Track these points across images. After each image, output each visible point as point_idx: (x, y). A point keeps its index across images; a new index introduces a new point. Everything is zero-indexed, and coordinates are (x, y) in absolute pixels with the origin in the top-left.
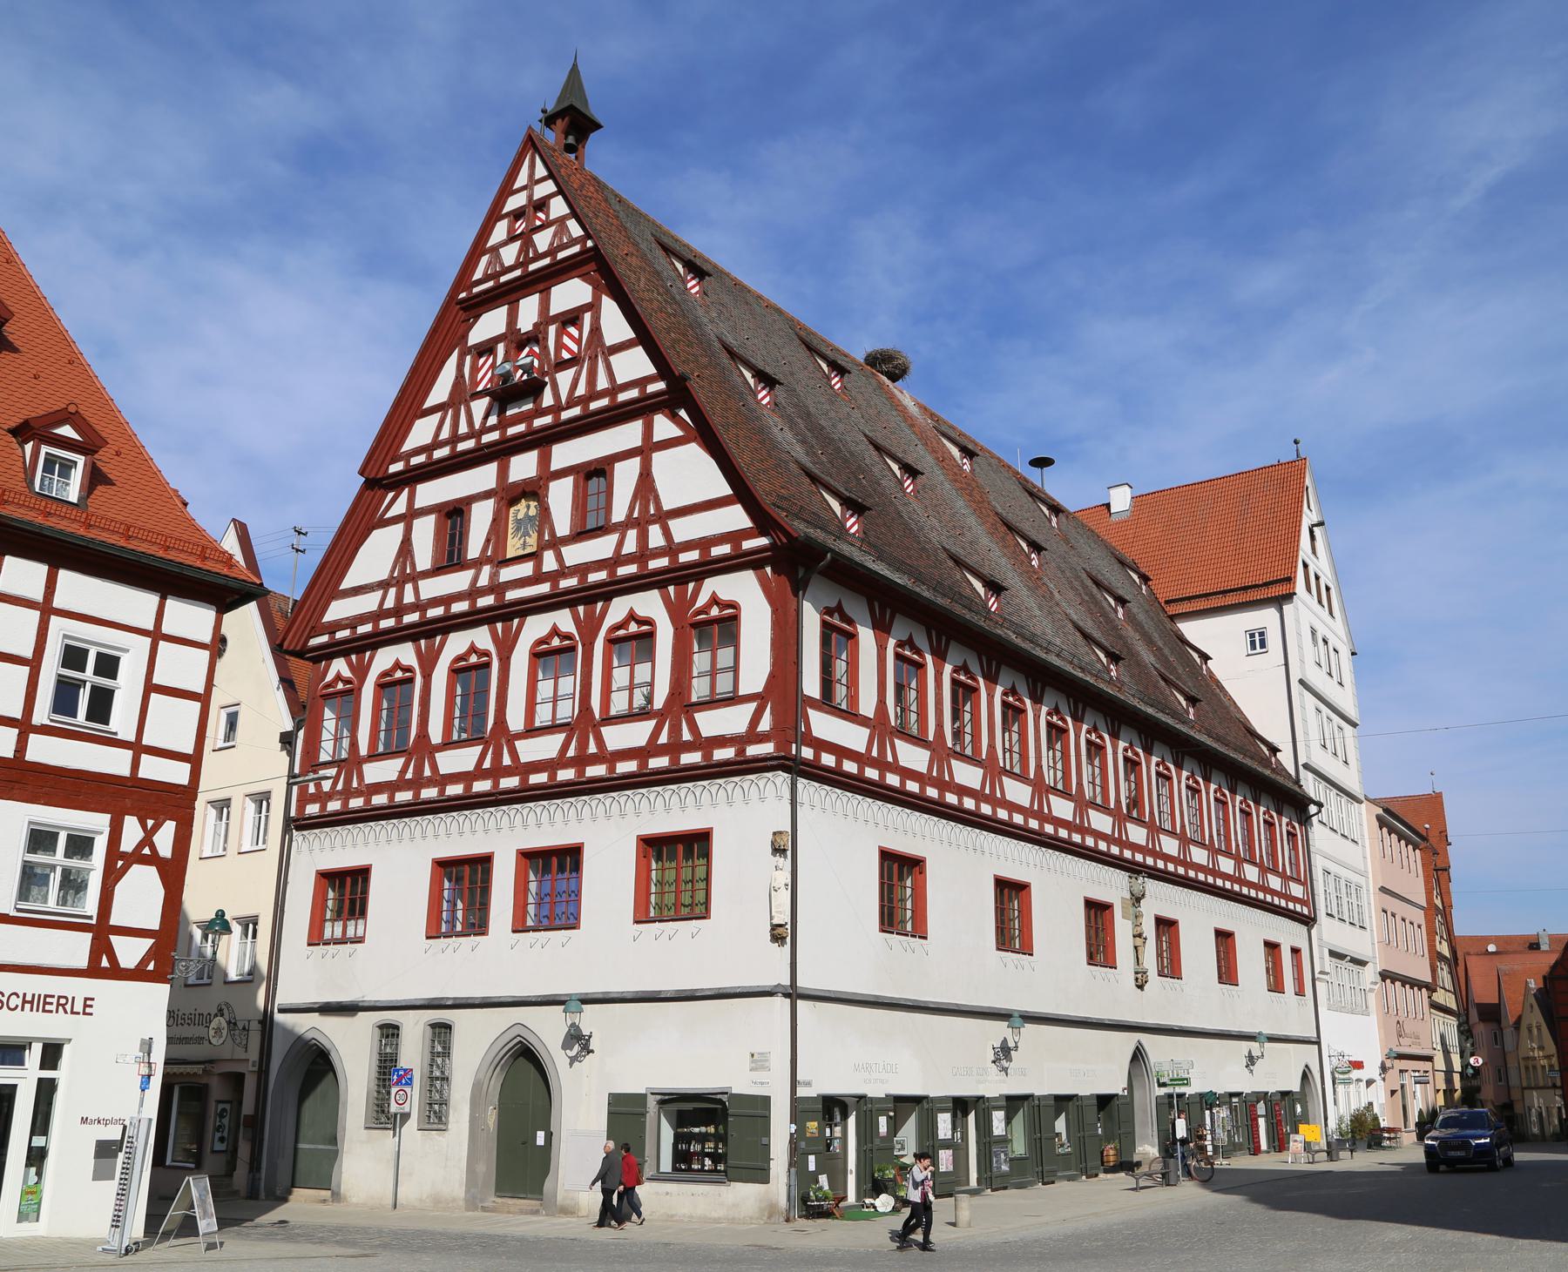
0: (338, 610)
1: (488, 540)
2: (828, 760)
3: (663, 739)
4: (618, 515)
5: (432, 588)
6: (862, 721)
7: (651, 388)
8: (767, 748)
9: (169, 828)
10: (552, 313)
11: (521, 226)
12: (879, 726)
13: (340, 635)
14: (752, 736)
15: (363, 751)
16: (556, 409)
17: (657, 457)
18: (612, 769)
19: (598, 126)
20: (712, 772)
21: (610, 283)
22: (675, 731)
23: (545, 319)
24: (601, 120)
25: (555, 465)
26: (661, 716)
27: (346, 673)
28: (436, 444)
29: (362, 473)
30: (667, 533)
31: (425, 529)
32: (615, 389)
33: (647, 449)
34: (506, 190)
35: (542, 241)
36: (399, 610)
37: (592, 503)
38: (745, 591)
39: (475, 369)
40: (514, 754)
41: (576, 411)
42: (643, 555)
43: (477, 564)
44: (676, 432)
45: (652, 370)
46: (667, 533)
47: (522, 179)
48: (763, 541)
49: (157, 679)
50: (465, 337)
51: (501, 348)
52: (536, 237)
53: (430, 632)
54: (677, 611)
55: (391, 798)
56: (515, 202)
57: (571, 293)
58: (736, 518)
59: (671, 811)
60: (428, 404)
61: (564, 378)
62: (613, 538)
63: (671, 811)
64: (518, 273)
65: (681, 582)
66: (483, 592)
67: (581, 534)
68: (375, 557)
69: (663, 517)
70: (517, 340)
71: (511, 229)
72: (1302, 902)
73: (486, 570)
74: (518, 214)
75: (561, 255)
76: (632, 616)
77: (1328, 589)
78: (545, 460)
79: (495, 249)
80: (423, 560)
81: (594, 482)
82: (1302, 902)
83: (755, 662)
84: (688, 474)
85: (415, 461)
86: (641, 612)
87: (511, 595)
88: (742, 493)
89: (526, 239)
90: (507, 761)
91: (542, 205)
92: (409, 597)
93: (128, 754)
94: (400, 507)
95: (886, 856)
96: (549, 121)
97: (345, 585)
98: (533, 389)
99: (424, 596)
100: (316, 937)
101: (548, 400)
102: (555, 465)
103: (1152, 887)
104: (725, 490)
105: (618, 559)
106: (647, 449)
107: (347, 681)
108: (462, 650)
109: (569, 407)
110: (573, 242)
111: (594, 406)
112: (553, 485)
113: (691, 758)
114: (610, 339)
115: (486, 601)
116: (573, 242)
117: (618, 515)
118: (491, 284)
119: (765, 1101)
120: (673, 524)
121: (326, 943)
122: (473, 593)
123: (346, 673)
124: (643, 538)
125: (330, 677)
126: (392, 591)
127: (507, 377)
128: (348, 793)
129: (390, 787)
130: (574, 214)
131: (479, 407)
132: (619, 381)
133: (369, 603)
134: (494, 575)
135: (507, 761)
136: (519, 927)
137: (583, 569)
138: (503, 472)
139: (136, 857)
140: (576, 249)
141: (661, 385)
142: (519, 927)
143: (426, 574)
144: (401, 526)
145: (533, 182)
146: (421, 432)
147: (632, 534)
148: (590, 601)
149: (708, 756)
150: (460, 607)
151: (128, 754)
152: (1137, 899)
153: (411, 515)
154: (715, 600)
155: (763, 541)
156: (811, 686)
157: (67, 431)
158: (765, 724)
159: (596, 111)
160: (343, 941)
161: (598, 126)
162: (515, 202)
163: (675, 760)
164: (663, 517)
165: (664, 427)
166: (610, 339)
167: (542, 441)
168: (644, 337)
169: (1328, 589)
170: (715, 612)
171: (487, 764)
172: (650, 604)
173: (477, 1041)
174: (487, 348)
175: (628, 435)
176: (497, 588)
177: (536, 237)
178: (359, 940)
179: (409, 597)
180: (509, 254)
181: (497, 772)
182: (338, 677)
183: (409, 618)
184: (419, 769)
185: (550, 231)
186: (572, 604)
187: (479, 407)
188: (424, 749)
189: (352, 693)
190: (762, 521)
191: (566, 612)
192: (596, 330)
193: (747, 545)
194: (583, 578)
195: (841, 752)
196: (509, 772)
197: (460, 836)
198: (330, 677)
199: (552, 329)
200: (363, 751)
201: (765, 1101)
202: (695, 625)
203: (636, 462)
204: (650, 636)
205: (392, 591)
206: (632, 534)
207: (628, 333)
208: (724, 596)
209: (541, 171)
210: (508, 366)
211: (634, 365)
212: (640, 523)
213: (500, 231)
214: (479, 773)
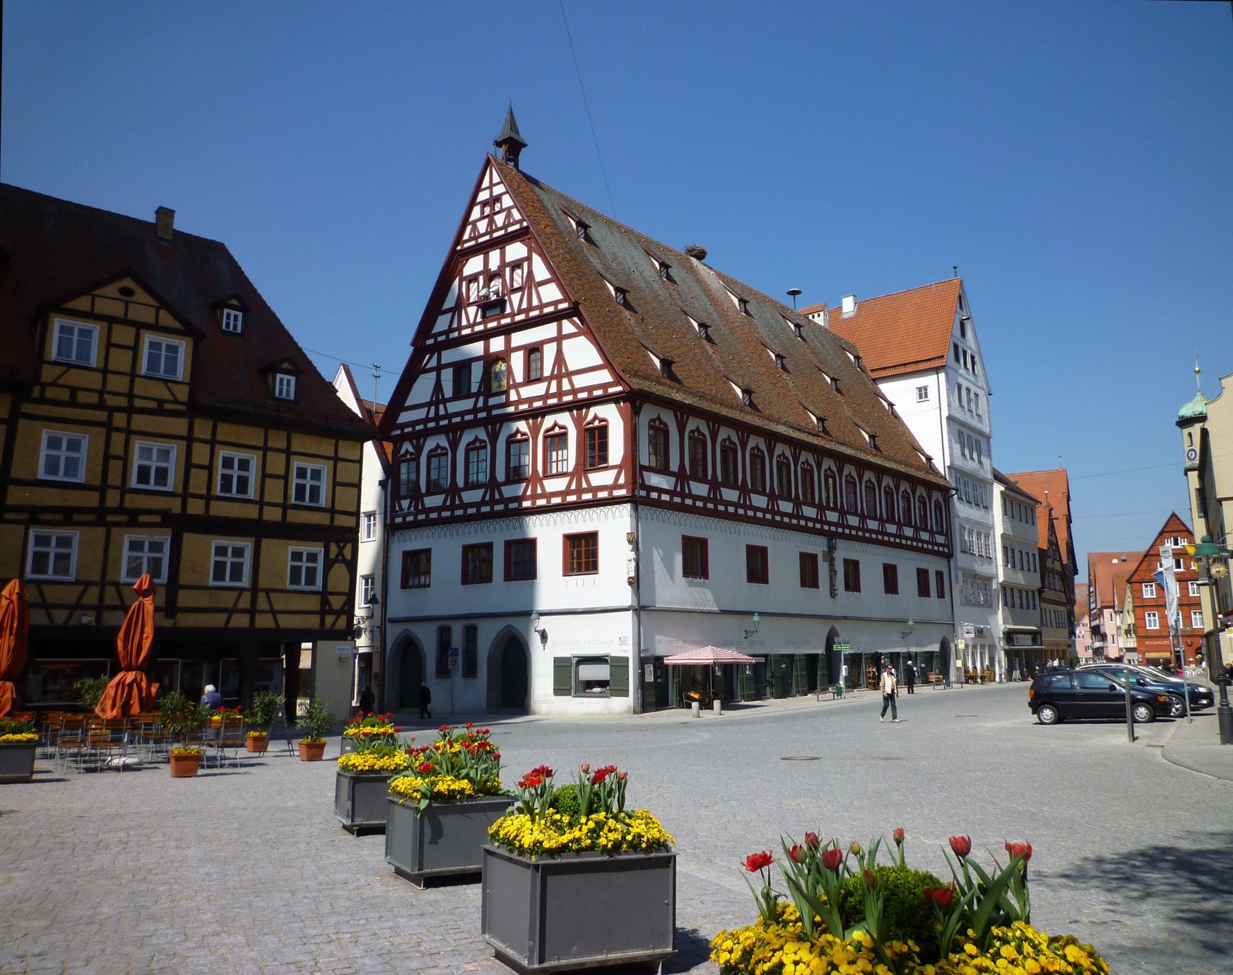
0: (404, 417)
1: (481, 383)
2: (654, 495)
3: (573, 487)
4: (547, 372)
5: (453, 407)
6: (672, 474)
7: (561, 306)
8: (623, 492)
9: (349, 546)
10: (507, 260)
11: (487, 210)
12: (681, 476)
13: (407, 430)
14: (616, 486)
15: (423, 491)
16: (513, 315)
17: (564, 342)
18: (549, 501)
19: (525, 145)
20: (596, 503)
21: (536, 246)
22: (579, 483)
23: (503, 264)
24: (526, 142)
25: (513, 345)
26: (572, 475)
27: (411, 450)
28: (451, 330)
29: (412, 345)
30: (571, 383)
31: (447, 375)
32: (542, 306)
33: (560, 338)
34: (478, 189)
35: (500, 220)
36: (437, 418)
37: (533, 366)
38: (612, 415)
39: (468, 289)
40: (500, 493)
41: (522, 317)
42: (560, 393)
43: (477, 395)
44: (575, 330)
45: (560, 296)
46: (571, 383)
47: (486, 183)
48: (620, 388)
49: (338, 480)
50: (461, 271)
51: (481, 278)
52: (496, 217)
53: (454, 431)
54: (578, 422)
55: (439, 515)
56: (484, 195)
57: (516, 251)
58: (605, 376)
59: (579, 522)
60: (444, 308)
61: (516, 298)
62: (545, 384)
63: (579, 522)
64: (487, 238)
65: (579, 408)
66: (481, 410)
67: (529, 381)
68: (422, 390)
69: (569, 374)
70: (490, 276)
71: (482, 212)
72: (943, 545)
73: (481, 398)
74: (484, 204)
75: (510, 229)
76: (556, 424)
77: (973, 358)
78: (508, 342)
79: (474, 223)
80: (448, 391)
81: (533, 356)
82: (943, 545)
83: (616, 449)
84: (581, 353)
85: (441, 338)
86: (560, 423)
87: (495, 412)
88: (608, 364)
89: (490, 218)
90: (497, 496)
91: (498, 199)
92: (442, 412)
93: (328, 515)
94: (433, 363)
95: (685, 538)
96: (498, 144)
97: (408, 403)
98: (500, 303)
99: (450, 411)
100: (405, 585)
101: (508, 310)
102: (513, 345)
103: (840, 543)
104: (599, 361)
105: (547, 396)
106: (560, 338)
107: (412, 454)
108: (471, 439)
109: (519, 314)
110: (516, 222)
111: (532, 314)
112: (514, 355)
113: (587, 496)
114: (538, 278)
115: (482, 415)
116: (516, 222)
117: (547, 372)
118: (473, 243)
119: (627, 659)
120: (574, 378)
121: (411, 587)
122: (475, 410)
123: (411, 450)
124: (559, 385)
125: (403, 451)
126: (433, 408)
127: (487, 297)
128: (418, 512)
129: (438, 509)
130: (515, 206)
131: (472, 310)
132: (544, 301)
133: (421, 414)
134: (486, 402)
135: (497, 496)
136: (508, 578)
137: (530, 400)
138: (487, 347)
139: (336, 560)
140: (517, 227)
141: (565, 305)
142: (508, 578)
143: (450, 400)
144: (433, 375)
145: (492, 185)
146: (442, 323)
147: (554, 383)
148: (535, 417)
149: (595, 495)
150: (469, 417)
151: (328, 515)
152: (832, 548)
153: (439, 368)
154: (596, 418)
155: (620, 388)
156: (644, 460)
157: (234, 302)
158: (622, 481)
159: (524, 136)
160: (419, 586)
161: (525, 145)
162: (484, 195)
163: (579, 497)
164: (569, 374)
165: (568, 327)
166: (538, 278)
167: (506, 331)
168: (555, 278)
169: (973, 358)
170: (596, 423)
171: (487, 498)
172: (565, 419)
173: (488, 635)
174: (473, 278)
175: (549, 330)
176: (486, 408)
177: (496, 217)
178: (429, 586)
179: (442, 412)
180: (482, 226)
181: (493, 502)
182: (407, 451)
183: (444, 422)
184: (453, 501)
185: (504, 214)
186: (526, 418)
187: (472, 310)
188: (453, 490)
189: (417, 460)
190: (619, 380)
191: (523, 422)
192: (530, 272)
193: (611, 390)
194: (531, 405)
195: (660, 491)
196: (498, 502)
197: (476, 534)
198: (403, 451)
199: (508, 270)
200: (423, 491)
201: (627, 659)
202: (586, 430)
203: (554, 344)
204: (565, 434)
205: (433, 408)
206: (554, 383)
207: (547, 275)
208: (600, 415)
209: (496, 179)
210: (483, 292)
211: (551, 293)
212: (558, 377)
213: (476, 213)
214: (483, 502)
